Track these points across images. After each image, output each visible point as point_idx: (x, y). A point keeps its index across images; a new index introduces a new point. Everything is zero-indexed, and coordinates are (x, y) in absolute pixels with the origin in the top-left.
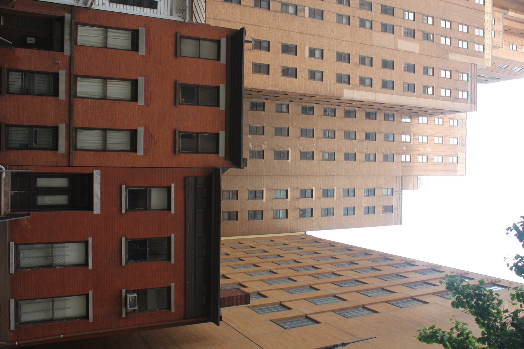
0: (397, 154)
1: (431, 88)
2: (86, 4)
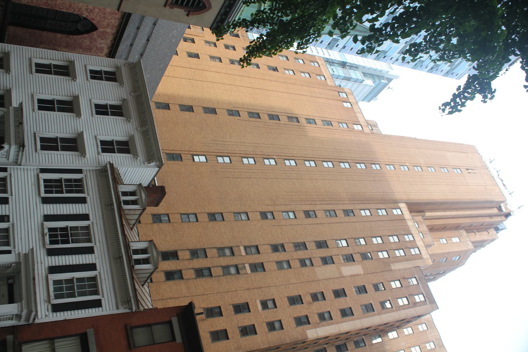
1: (388, 302)
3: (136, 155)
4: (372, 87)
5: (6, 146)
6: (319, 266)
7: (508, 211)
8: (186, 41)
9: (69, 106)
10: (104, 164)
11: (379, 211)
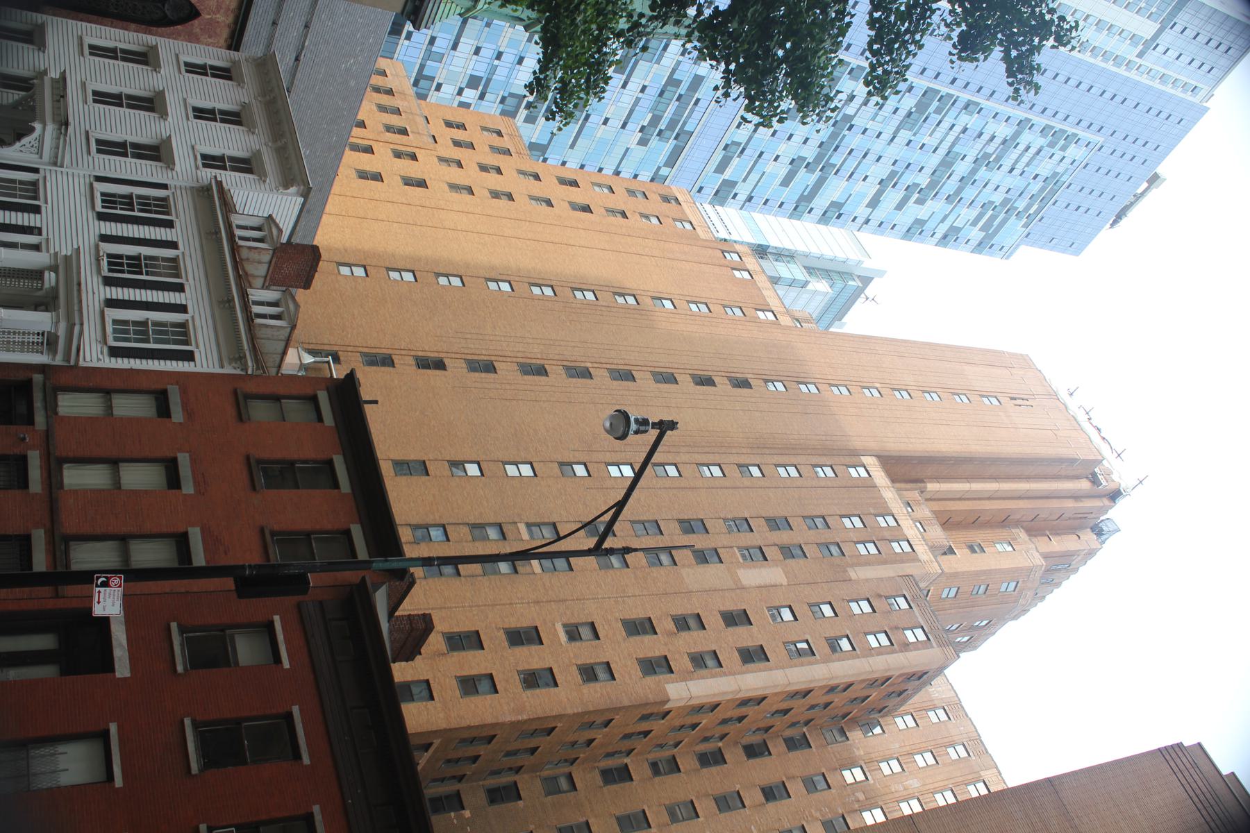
0: (848, 812)
1: (845, 640)
4: (828, 297)
5: (38, 126)
6: (689, 566)
7: (1112, 486)
10: (206, 183)
11: (819, 469)
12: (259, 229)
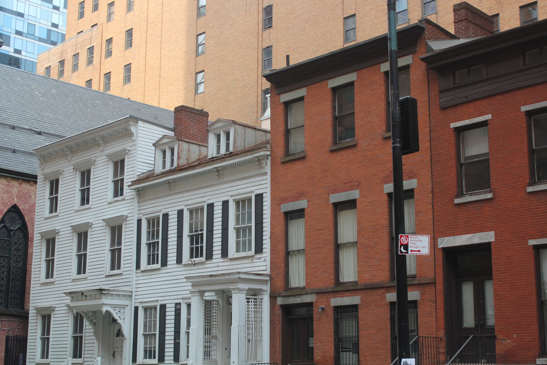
2: (267, 281)
3: (125, 152)
5: (104, 309)
8: (111, 52)
9: (82, 236)
12: (164, 152)
